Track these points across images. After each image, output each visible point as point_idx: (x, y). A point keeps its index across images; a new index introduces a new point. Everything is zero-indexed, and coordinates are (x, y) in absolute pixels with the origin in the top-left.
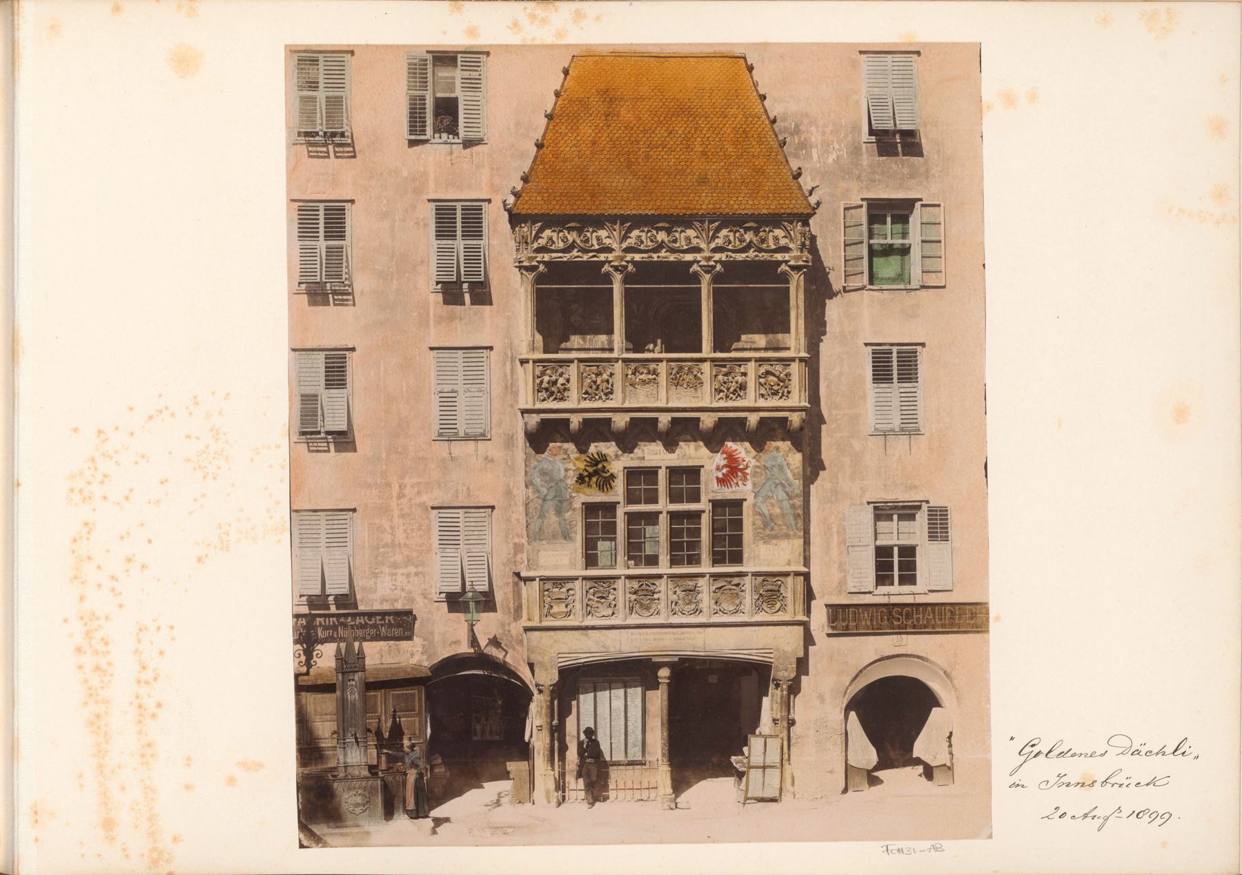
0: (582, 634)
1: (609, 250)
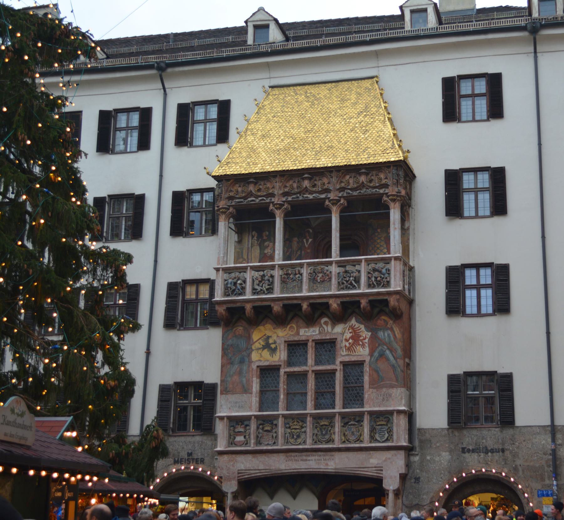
0: (254, 457)
1: (272, 195)
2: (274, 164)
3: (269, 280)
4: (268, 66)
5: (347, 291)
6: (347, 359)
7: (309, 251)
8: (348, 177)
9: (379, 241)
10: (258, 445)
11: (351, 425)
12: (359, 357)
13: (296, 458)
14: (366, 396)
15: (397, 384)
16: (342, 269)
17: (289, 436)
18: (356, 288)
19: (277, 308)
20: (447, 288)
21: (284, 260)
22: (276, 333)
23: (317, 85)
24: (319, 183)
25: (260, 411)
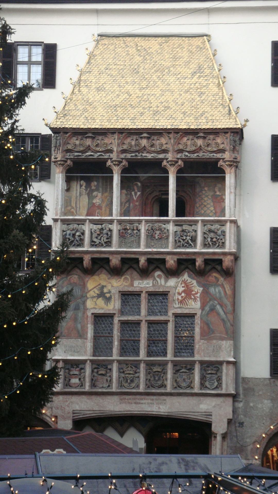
0: (88, 399)
1: (111, 151)
2: (112, 121)
3: (107, 234)
4: (97, 11)
5: (183, 249)
6: (179, 311)
7: (137, 204)
8: (185, 139)
9: (206, 199)
10: (93, 387)
11: (183, 372)
12: (191, 310)
13: (130, 401)
14: (197, 346)
15: (226, 337)
16: (179, 229)
17: (123, 381)
18: (192, 247)
19: (115, 261)
20: (271, 248)
21: (121, 216)
22: (110, 283)
23: (147, 38)
24: (157, 143)
25: (93, 356)
